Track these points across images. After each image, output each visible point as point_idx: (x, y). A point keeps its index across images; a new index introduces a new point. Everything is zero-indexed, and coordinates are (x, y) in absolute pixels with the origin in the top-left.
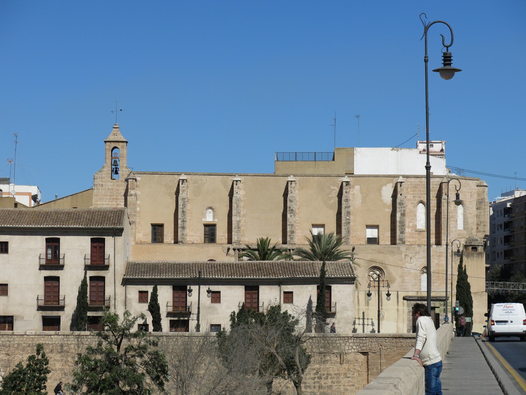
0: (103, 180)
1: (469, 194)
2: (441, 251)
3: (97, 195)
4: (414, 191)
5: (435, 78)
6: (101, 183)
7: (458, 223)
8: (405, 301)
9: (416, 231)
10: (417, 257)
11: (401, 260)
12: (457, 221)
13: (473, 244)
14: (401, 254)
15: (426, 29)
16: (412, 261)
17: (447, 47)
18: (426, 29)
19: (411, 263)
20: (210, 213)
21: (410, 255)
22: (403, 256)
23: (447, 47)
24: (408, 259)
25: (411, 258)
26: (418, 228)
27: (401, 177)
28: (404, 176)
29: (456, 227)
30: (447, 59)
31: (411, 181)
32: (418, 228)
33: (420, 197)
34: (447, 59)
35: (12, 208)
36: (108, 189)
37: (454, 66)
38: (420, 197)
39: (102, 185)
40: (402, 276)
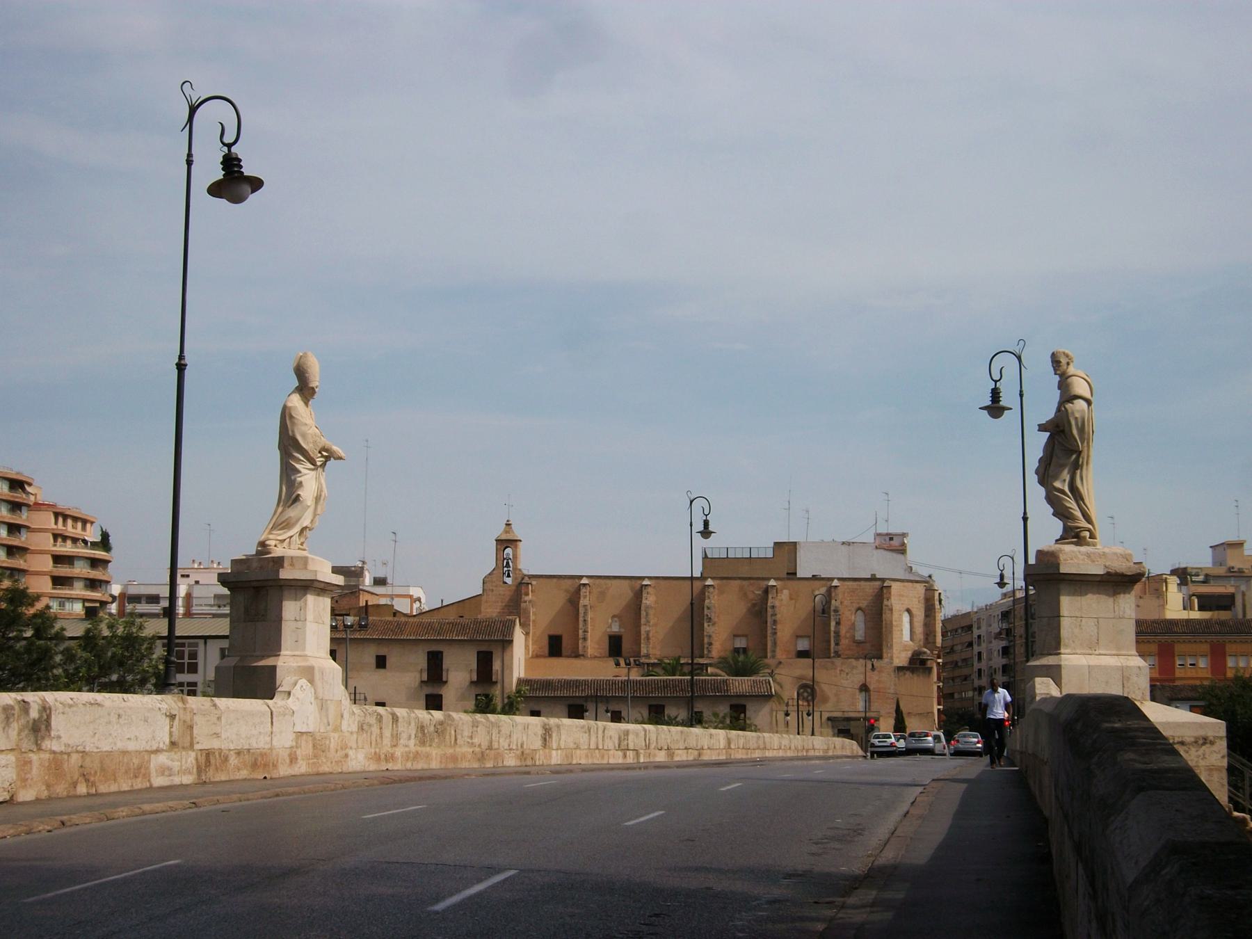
0: (494, 584)
1: (917, 600)
2: (882, 665)
3: (487, 602)
4: (851, 596)
5: (698, 538)
6: (491, 588)
7: (904, 632)
8: (830, 723)
9: (854, 642)
10: (855, 671)
11: (836, 676)
12: (902, 630)
13: (921, 657)
14: (835, 669)
15: (691, 502)
16: (848, 677)
17: (706, 515)
18: (691, 502)
19: (847, 679)
20: (616, 621)
21: (847, 671)
22: (838, 672)
23: (706, 515)
24: (844, 675)
25: (847, 674)
26: (856, 638)
27: (836, 581)
28: (839, 579)
29: (901, 637)
30: (706, 523)
31: (848, 585)
32: (856, 638)
33: (859, 603)
34: (706, 523)
35: (391, 618)
36: (500, 595)
37: (711, 529)
38: (859, 603)
39: (492, 590)
40: (836, 695)
